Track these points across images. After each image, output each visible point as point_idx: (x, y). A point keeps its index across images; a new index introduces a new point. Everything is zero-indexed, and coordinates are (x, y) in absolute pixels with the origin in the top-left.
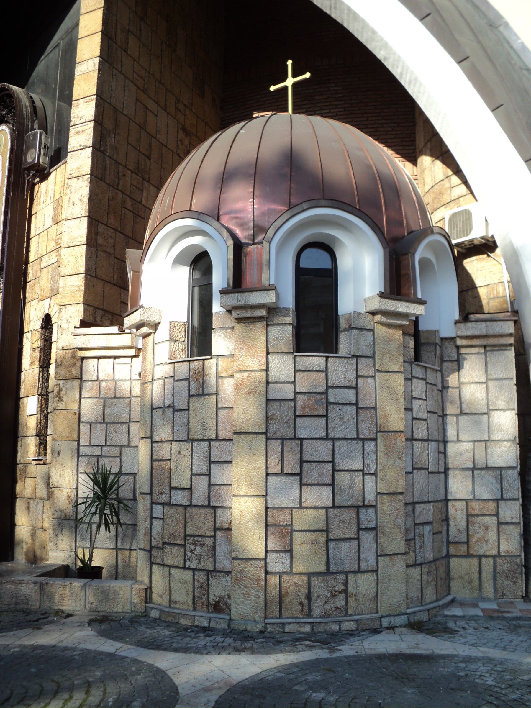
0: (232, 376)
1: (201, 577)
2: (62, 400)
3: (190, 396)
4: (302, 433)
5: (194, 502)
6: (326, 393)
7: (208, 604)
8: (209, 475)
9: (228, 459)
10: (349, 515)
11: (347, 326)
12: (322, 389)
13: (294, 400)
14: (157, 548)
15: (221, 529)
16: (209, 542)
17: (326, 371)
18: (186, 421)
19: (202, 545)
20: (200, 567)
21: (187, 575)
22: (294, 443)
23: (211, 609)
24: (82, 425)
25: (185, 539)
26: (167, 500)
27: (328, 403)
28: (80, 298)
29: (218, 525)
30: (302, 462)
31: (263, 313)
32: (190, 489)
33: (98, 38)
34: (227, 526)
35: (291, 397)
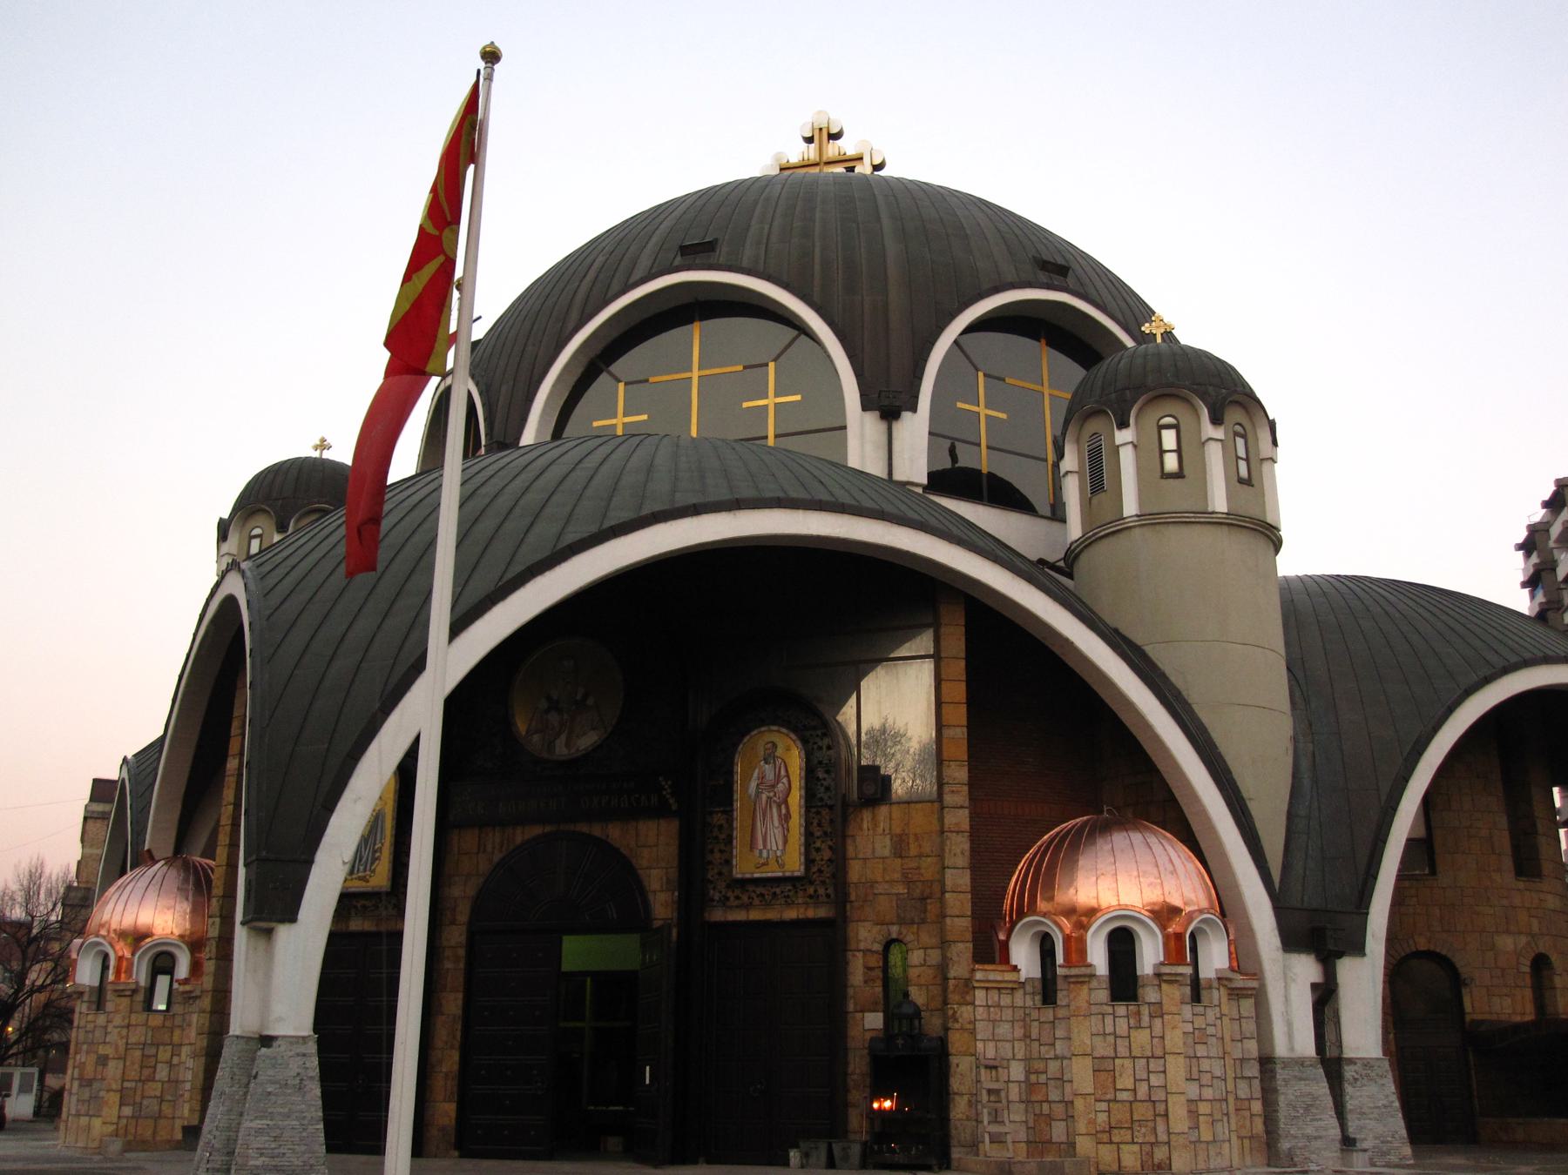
0: (1162, 1016)
1: (1147, 1148)
2: (958, 1022)
3: (1130, 1028)
5: (1138, 1098)
6: (1205, 1029)
7: (1154, 1165)
8: (1148, 1080)
9: (1162, 1069)
10: (1217, 1105)
11: (1207, 986)
12: (1204, 1026)
13: (1193, 1033)
14: (1104, 1132)
15: (1160, 1115)
16: (1151, 1124)
18: (1127, 1044)
19: (1146, 1126)
20: (1145, 1141)
21: (1136, 1148)
22: (1194, 1060)
23: (1155, 1168)
24: (978, 1043)
25: (1132, 1124)
26: (1112, 1098)
28: (969, 936)
29: (1157, 1112)
32: (1135, 1090)
33: (963, 709)
34: (1163, 1113)
35: (1191, 1030)
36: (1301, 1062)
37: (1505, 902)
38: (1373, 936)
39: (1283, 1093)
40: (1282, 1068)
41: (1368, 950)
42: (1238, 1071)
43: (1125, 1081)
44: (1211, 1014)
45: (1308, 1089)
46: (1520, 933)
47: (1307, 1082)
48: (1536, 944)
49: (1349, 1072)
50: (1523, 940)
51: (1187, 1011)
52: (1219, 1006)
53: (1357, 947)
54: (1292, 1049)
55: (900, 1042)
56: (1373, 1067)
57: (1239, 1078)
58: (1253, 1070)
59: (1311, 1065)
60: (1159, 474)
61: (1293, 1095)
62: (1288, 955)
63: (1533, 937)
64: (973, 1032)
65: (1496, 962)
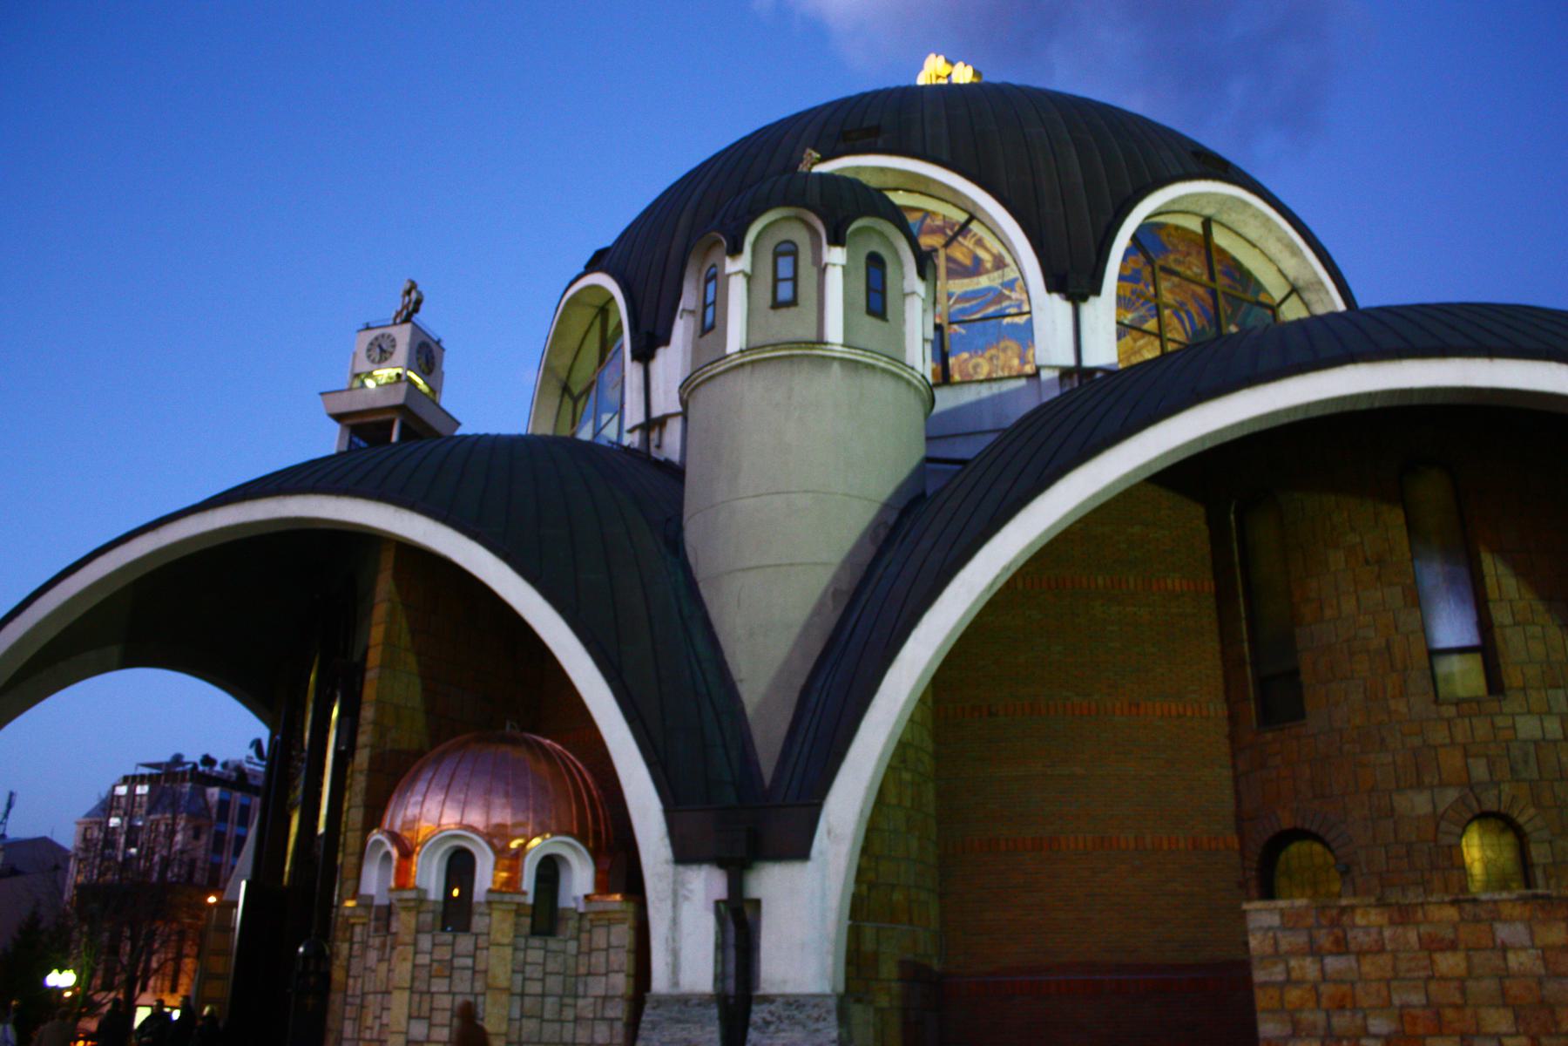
4: (434, 989)
6: (451, 961)
12: (448, 957)
13: (430, 965)
17: (453, 944)
22: (427, 997)
27: (452, 968)
30: (432, 1009)
31: (412, 904)
36: (684, 1001)
37: (1416, 741)
38: (829, 833)
39: (644, 1039)
40: (654, 1008)
41: (815, 852)
42: (599, 1008)
43: (369, 1021)
44: (465, 943)
45: (685, 1034)
46: (1443, 785)
47: (688, 1025)
48: (1479, 801)
49: (758, 1013)
50: (1452, 795)
51: (425, 942)
52: (488, 934)
53: (798, 848)
54: (676, 984)
55: (312, 980)
56: (804, 1006)
57: (599, 1019)
58: (618, 1011)
59: (699, 1005)
60: (699, 333)
61: (659, 1041)
62: (681, 868)
63: (1471, 789)
64: (348, 970)
65: (1396, 835)
